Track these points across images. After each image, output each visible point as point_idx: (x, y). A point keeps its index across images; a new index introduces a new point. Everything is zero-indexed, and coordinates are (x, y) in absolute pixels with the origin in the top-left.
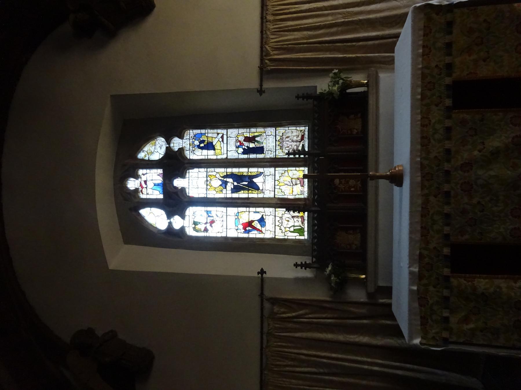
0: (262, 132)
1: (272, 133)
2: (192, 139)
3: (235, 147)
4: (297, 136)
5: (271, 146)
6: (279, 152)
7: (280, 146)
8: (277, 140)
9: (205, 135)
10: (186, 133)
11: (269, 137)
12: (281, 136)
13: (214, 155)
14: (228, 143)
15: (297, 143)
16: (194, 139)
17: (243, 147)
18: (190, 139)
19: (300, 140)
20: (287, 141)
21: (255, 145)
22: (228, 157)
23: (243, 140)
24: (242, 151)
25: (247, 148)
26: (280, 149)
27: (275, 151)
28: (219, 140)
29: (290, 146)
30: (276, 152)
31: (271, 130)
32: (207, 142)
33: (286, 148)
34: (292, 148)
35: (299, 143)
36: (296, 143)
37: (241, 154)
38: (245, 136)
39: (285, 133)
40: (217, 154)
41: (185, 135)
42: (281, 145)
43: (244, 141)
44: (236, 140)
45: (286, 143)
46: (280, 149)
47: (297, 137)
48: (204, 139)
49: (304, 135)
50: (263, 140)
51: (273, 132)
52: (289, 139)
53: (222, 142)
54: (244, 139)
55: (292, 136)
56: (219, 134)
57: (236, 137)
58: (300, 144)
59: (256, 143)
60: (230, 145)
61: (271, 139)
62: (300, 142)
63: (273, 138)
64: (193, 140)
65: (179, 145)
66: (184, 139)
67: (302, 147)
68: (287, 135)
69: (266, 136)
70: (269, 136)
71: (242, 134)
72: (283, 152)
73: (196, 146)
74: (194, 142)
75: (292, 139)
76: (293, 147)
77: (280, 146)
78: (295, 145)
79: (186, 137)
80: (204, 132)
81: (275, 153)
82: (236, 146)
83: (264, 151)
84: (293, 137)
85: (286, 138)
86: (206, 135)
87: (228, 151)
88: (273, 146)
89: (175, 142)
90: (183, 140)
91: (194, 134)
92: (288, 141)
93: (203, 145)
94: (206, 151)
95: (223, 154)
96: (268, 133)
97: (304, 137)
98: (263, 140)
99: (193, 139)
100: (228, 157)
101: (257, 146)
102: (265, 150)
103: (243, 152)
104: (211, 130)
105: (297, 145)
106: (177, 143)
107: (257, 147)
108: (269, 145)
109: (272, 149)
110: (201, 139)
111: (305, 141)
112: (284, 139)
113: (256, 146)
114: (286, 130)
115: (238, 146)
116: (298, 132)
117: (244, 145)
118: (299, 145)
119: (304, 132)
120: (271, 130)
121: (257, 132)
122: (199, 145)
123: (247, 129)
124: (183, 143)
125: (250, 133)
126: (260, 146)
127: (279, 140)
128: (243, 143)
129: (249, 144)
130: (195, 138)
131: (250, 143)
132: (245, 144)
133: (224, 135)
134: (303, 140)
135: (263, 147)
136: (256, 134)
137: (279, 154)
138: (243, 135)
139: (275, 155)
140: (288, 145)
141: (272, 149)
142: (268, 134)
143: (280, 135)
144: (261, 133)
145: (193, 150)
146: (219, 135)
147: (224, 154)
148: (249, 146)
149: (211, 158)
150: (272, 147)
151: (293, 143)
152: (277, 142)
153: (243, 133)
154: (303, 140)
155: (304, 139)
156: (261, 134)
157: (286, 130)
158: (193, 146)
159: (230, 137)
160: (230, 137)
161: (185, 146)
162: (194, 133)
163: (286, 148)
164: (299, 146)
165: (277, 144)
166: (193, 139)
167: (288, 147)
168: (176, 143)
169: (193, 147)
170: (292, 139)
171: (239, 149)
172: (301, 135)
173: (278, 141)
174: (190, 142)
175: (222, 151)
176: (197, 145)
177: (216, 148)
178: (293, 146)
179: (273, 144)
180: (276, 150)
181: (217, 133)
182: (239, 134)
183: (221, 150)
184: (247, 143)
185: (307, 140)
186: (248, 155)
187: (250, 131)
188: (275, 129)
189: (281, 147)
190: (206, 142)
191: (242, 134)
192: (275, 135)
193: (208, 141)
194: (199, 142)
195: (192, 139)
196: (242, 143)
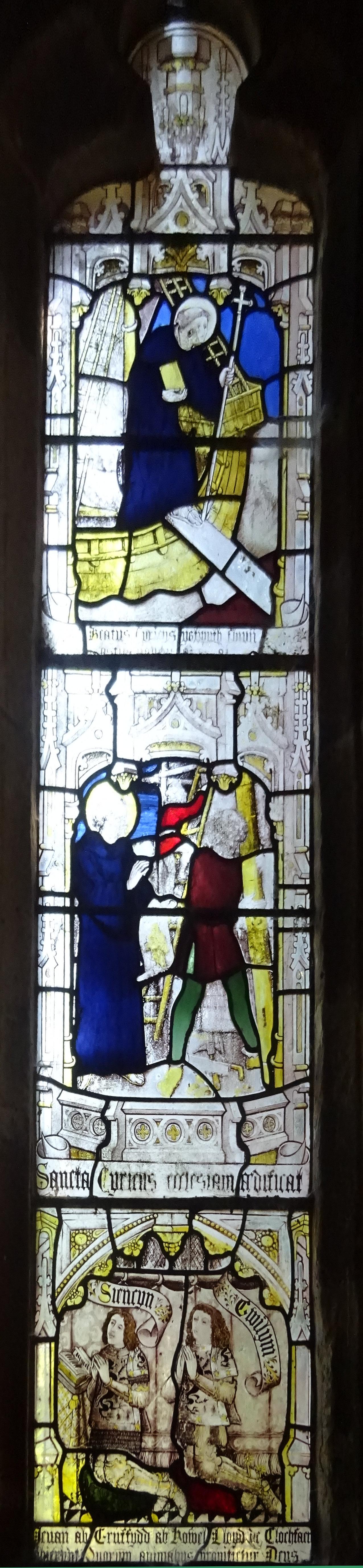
0: (273, 1052)
1: (263, 1170)
2: (229, 274)
3: (146, 758)
4: (231, 1437)
5: (153, 1153)
6: (91, 1239)
7: (144, 1251)
8: (196, 1225)
9: (267, 419)
10: (289, 201)
11: (232, 1130)
12: (231, 1269)
13: (75, 518)
14: (192, 680)
15: (165, 1443)
16: (235, 293)
17: (145, 849)
18: (238, 249)
19: (190, 1473)
20: (186, 1324)
21: (155, 979)
22: (52, 677)
23: (207, 842)
24: (110, 837)
25: (132, 884)
26: (117, 1253)
27: (98, 1192)
28: (213, 569)
29: (143, 1358)
30: (92, 1203)
31: (291, 1148)
32: (204, 441)
33: (125, 1312)
34: (122, 1387)
35: (164, 1460)
36: (164, 1425)
37: (82, 817)
38: (249, 869)
39: (261, 1312)
40: (81, 548)
41: (272, 195)
42: (149, 1265)
43: (203, 854)
44: (210, 766)
45: (168, 1319)
46: (117, 1253)
47: (223, 1438)
48: (226, 409)
49: (239, 1511)
50: (202, 1062)
51: (279, 1170)
52: (205, 1346)
53: (191, 605)
54: (220, 851)
55: (234, 1380)
56: (275, 574)
57: (241, 770)
58: (153, 1469)
59: (178, 984)
60: (166, 703)
61: (209, 1149)
62: (175, 1472)
63: (214, 1180)
64: (226, 283)
65: (184, 122)
66: (238, 183)
67: (129, 1494)
68: (240, 1332)
69: (240, 1101)
70: (240, 1126)
71: (264, 831)
72: (84, 1283)
73: (163, 321)
74: (206, 294)
75: (204, 1380)
76: (126, 1397)
77: (144, 1251)
78: (150, 1409)
79: (251, 204)
80: (293, 407)
81: (84, 1193)
82: (157, 763)
83: (103, 1072)
84: (226, 1391)
85: (218, 1322)
86: (270, 430)
87: (107, 675)
88: (145, 1178)
89: (209, 77)
90: (225, 174)
91: (279, 286)
92: (191, 1341)
93: (169, 396)
94: (116, 426)
95: (85, 614)
96: (269, 1123)
97: (218, 1519)
98: (202, 1062)
99: (236, 283)
100: (52, 677)
101: (151, 994)
102: (114, 1087)
103: (97, 835)
104: (306, 490)
105: (148, 1442)
106: (200, 105)
107: (141, 1001)
108: (158, 1131)
109: (115, 1167)
110: (227, 375)
111: (184, 1523)
112: (205, 1296)
113: (147, 982)
114: (288, 1318)
115: (155, 789)
116: (261, 1444)
117: (159, 856)
118: (147, 1457)
119: (268, 1514)
120: (291, 1148)
121: (277, 994)
122: (173, 352)
123: (310, 888)
124: (199, 173)
125: (269, 921)
126: (147, 1031)
127: (202, 1239)
128: (185, 839)
129: (171, 905)
130: (241, 301)
131: (180, 919)
132: (170, 860)
133: (259, 632)
134: (195, 1508)
135: (143, 1068)
136: (259, 981)
137: (73, 1243)
138: (258, 850)
139: (63, 1193)
140: (147, 1342)
141: (115, 1167)
142: (258, 1120)
143: (242, 1252)
144: (266, 1049)
145: (124, 284)
146: (262, 578)
147: (82, 624)
148: (154, 904)
149: (50, 483)
150: (134, 1169)
151: (169, 1389)
152: (180, 1218)
153: (274, 848)
154: (195, 1508)
155: (204, 1519)
156: (257, 1050)
157: (288, 1318)
158: (164, 284)
159: (239, 699)
160: (239, 699)
161: (170, 198)
162: (283, 294)
163: (118, 1319)
164: (135, 1457)
165: (163, 1218)
166: (236, 283)
167: (132, 1343)
168: (198, 90)
169: (153, 279)
170: (204, 1380)
171: (130, 797)
172: (241, 1479)
173: (192, 1233)
174: (206, 250)
175: (116, 610)
176: (170, 328)
177: (144, 539)
178: (139, 1395)
179: (160, 1172)
180: (109, 1204)
181: (280, 552)
182: (270, 795)
183: (120, 596)
184: (181, 893)
185: (190, 1550)
186: (70, 895)
187: (288, 922)
188: (304, 1193)
189: (130, 1259)
190: (205, 430)
191: (264, 831)
192: (243, 1194)
193: (215, 443)
194: (200, 350)
195: (229, 274)
196: (187, 829)
